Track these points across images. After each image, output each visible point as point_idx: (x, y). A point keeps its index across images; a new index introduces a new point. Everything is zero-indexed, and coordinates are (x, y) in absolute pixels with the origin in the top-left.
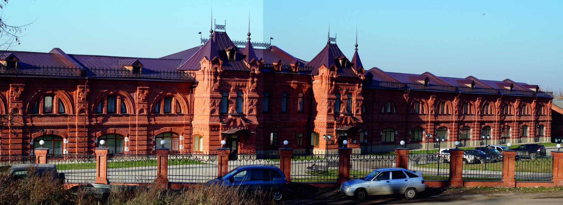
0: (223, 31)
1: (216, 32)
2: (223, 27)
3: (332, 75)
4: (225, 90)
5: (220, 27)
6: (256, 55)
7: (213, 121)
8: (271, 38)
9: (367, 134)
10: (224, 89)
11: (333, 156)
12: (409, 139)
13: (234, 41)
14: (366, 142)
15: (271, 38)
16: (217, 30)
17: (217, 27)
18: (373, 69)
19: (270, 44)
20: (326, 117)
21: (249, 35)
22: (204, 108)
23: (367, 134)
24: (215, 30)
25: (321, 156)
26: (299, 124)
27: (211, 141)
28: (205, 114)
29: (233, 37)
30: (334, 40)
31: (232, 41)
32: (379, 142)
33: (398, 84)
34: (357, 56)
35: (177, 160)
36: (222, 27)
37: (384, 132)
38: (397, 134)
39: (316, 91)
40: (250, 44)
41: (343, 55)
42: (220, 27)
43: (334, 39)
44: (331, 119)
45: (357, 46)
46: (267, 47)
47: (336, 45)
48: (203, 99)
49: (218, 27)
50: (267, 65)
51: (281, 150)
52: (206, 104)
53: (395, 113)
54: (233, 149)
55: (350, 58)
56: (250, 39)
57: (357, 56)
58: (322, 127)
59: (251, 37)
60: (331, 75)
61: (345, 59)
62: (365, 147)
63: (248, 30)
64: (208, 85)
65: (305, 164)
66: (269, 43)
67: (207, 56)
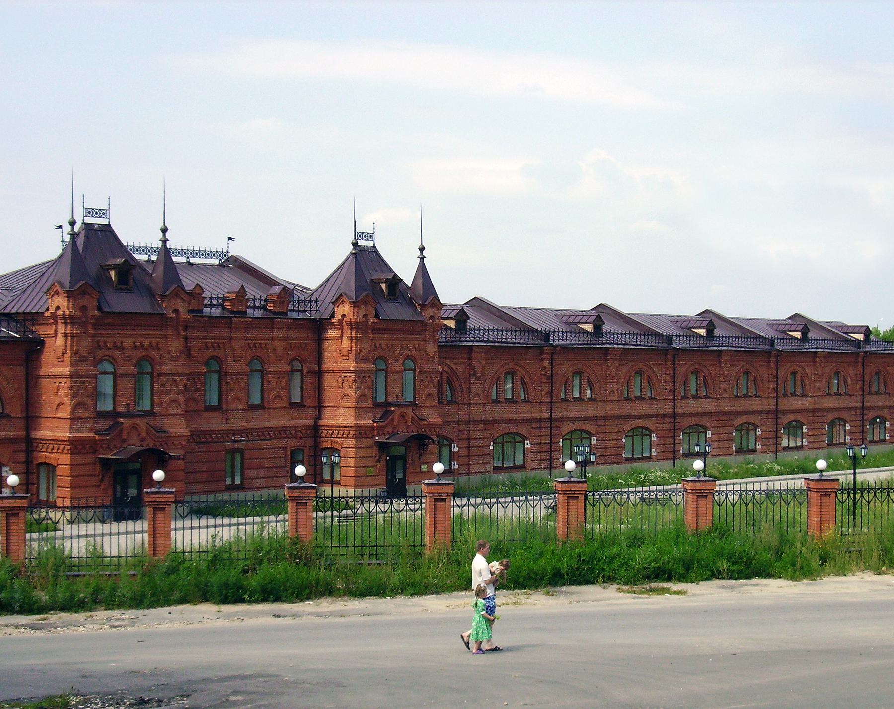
0: (105, 222)
1: (88, 227)
2: (104, 214)
3: (365, 316)
4: (107, 358)
5: (96, 213)
6: (182, 277)
7: (80, 431)
8: (230, 239)
9: (456, 449)
10: (104, 356)
11: (366, 500)
12: (558, 459)
13: (130, 244)
14: (457, 467)
15: (230, 239)
16: (89, 220)
17: (89, 213)
18: (474, 301)
19: (228, 252)
20: (353, 413)
21: (164, 231)
22: (57, 400)
23: (456, 449)
24: (84, 220)
25: (351, 500)
26: (293, 432)
27: (74, 476)
28: (60, 415)
29: (127, 236)
30: (370, 237)
31: (125, 244)
32: (488, 466)
33: (577, 335)
34: (422, 271)
35: (81, 519)
36: (102, 213)
37: (498, 443)
38: (529, 446)
39: (329, 355)
40: (166, 252)
41: (391, 270)
42: (96, 213)
43: (369, 236)
44: (364, 418)
45: (422, 249)
46: (220, 260)
47: (374, 250)
48: (55, 380)
49: (91, 212)
50: (211, 298)
51: (289, 488)
52: (61, 393)
53: (523, 401)
54: (130, 495)
55: (407, 275)
56: (165, 241)
57: (422, 271)
58: (344, 436)
59: (168, 235)
60: (361, 317)
61: (395, 281)
62: (68, 487)
63: (71, 212)
64: (66, 346)
65: (105, 532)
66: (225, 250)
67: (63, 281)
